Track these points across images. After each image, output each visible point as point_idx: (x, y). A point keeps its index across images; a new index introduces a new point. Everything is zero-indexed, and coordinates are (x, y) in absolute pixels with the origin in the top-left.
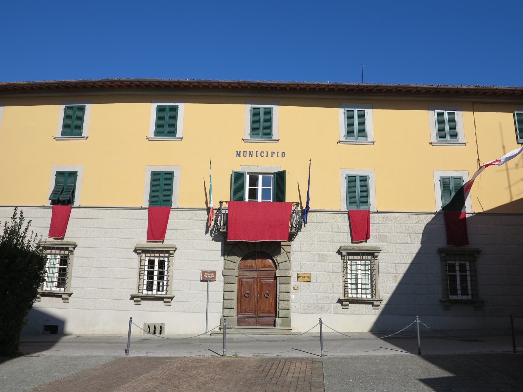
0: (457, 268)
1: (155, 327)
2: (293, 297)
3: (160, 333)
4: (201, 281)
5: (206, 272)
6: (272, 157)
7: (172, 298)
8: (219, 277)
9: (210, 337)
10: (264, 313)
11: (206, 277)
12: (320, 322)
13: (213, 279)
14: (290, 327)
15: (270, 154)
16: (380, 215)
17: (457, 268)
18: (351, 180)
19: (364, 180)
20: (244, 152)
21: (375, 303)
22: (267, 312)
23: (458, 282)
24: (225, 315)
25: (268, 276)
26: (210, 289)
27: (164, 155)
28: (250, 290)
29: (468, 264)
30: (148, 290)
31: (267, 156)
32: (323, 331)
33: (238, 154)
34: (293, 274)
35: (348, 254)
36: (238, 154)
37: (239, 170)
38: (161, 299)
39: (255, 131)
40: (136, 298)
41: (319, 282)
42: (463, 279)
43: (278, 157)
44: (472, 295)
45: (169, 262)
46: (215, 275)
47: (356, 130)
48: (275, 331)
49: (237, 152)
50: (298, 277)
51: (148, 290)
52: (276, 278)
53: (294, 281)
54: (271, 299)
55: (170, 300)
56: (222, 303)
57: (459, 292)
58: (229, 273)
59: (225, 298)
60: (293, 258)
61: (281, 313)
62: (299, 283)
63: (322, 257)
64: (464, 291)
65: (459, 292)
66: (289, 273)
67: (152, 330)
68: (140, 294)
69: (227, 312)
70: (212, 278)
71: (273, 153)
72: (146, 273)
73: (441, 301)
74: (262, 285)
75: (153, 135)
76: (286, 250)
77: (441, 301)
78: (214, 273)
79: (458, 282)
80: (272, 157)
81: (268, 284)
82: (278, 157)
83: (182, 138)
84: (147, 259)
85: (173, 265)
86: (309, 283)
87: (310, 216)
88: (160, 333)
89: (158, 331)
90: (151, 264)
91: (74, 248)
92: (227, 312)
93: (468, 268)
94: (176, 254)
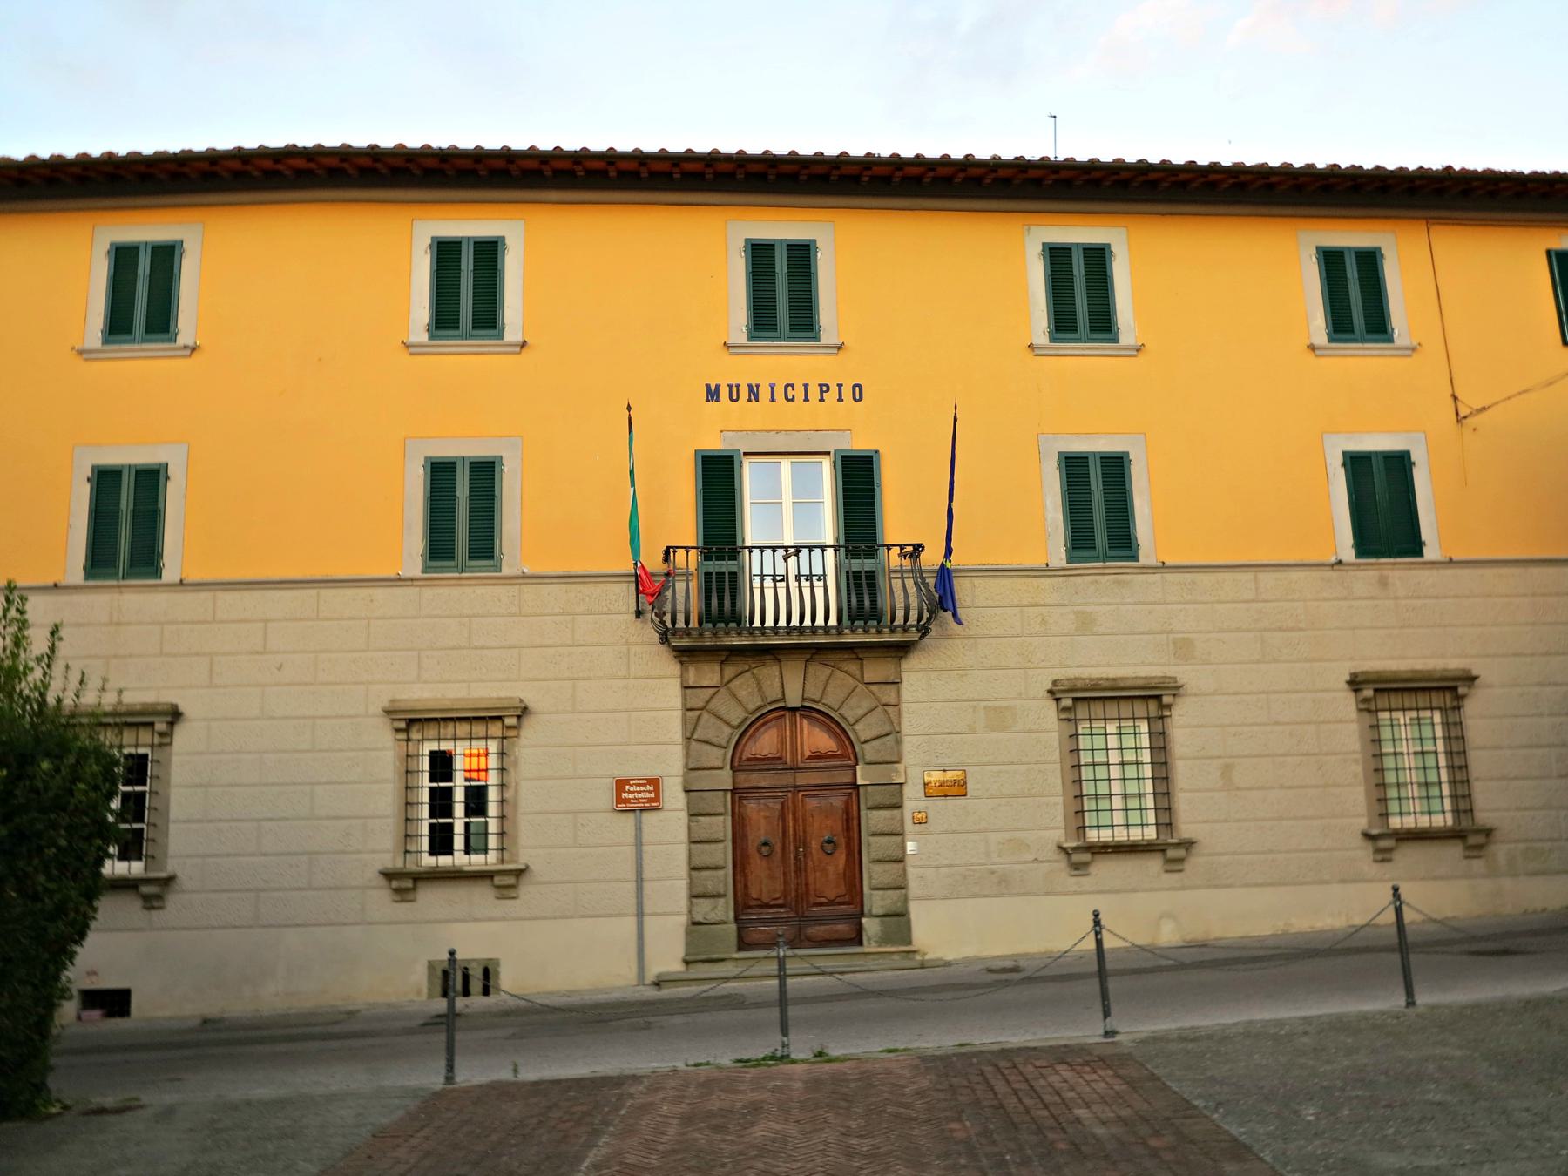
2: (910, 847)
5: (626, 782)
6: (822, 400)
7: (519, 873)
8: (674, 795)
9: (652, 994)
10: (821, 904)
12: (1097, 923)
14: (910, 943)
15: (814, 392)
16: (1172, 577)
19: (1116, 466)
20: (730, 386)
21: (1171, 853)
22: (831, 903)
24: (699, 918)
30: (434, 851)
31: (806, 399)
32: (1107, 945)
33: (713, 394)
36: (713, 394)
37: (714, 444)
39: (762, 321)
41: (991, 797)
43: (840, 399)
46: (657, 791)
48: (858, 962)
49: (708, 386)
55: (511, 880)
58: (704, 781)
59: (697, 862)
60: (906, 727)
62: (931, 802)
63: (999, 718)
66: (897, 771)
69: (704, 909)
70: (650, 800)
71: (824, 388)
73: (1367, 836)
78: (655, 782)
80: (822, 400)
82: (840, 399)
83: (524, 344)
85: (516, 763)
86: (961, 801)
88: (486, 992)
89: (476, 985)
91: (172, 724)
92: (704, 909)
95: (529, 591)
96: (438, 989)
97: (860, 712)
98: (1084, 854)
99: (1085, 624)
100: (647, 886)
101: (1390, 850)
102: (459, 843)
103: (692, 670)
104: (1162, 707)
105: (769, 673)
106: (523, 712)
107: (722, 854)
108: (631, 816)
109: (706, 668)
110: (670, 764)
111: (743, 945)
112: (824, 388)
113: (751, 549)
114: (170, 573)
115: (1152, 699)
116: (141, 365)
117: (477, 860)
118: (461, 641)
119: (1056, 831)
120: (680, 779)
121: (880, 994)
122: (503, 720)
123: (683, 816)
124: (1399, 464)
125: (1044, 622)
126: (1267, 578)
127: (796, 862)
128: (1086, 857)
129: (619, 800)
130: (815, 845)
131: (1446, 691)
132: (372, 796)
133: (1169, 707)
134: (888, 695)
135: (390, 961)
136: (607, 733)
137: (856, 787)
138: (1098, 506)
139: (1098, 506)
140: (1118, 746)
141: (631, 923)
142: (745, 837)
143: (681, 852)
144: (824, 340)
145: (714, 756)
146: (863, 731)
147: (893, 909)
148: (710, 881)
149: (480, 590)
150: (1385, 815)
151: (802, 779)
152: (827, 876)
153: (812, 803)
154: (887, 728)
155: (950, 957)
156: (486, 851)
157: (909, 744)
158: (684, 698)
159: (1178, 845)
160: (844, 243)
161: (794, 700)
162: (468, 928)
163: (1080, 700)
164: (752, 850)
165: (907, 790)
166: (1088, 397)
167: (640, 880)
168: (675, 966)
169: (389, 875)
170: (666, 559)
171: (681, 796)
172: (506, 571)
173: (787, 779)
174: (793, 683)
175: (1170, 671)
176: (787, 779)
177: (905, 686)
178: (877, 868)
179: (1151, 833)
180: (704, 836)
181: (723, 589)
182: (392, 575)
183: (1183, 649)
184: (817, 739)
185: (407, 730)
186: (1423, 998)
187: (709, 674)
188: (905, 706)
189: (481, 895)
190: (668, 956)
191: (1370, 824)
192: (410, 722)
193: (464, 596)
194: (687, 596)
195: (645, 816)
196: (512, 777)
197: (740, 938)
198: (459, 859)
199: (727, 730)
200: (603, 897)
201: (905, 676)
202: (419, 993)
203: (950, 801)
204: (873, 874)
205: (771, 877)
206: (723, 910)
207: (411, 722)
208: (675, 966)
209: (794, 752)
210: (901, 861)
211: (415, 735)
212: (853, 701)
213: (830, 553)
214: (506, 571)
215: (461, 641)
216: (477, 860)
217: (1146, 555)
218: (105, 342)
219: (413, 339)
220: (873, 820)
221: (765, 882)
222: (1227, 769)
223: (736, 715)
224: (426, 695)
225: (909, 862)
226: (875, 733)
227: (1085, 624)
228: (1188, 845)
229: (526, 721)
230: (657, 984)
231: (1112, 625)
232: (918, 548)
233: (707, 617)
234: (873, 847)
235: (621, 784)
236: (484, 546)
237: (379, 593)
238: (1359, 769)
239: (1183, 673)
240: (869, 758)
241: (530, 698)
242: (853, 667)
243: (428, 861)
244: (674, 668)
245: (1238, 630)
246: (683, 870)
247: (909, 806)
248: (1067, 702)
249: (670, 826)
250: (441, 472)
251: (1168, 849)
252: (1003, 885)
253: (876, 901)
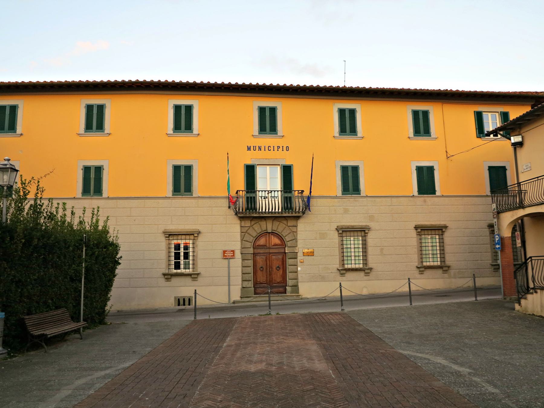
1: (184, 299)
2: (299, 269)
3: (189, 304)
5: (226, 251)
7: (198, 274)
8: (238, 255)
9: (233, 305)
11: (228, 255)
12: (340, 285)
15: (276, 148)
16: (369, 199)
18: (344, 169)
19: (355, 169)
21: (366, 271)
33: (249, 149)
36: (249, 149)
37: (249, 163)
39: (262, 129)
40: (168, 276)
45: (193, 244)
46: (234, 253)
51: (185, 268)
53: (300, 257)
55: (196, 276)
58: (246, 251)
59: (244, 272)
60: (299, 237)
62: (304, 257)
63: (323, 236)
67: (182, 302)
68: (170, 273)
69: (246, 284)
72: (173, 254)
73: (417, 267)
75: (171, 132)
76: (293, 230)
83: (198, 135)
85: (197, 246)
86: (312, 257)
87: (313, 202)
88: (189, 304)
89: (187, 303)
90: (177, 247)
92: (246, 284)
95: (200, 201)
96: (177, 304)
97: (287, 234)
98: (344, 271)
99: (346, 211)
100: (231, 278)
101: (423, 271)
102: (182, 266)
103: (243, 222)
104: (365, 233)
106: (199, 233)
107: (250, 270)
108: (226, 261)
109: (247, 222)
110: (237, 246)
111: (255, 293)
113: (259, 191)
114: (105, 195)
115: (362, 231)
116: (94, 138)
117: (187, 271)
118: (183, 214)
119: (336, 264)
120: (239, 251)
121: (290, 304)
122: (194, 234)
123: (240, 260)
124: (431, 170)
125: (335, 210)
126: (394, 200)
127: (270, 272)
128: (344, 272)
129: (224, 256)
130: (274, 268)
131: (440, 230)
132: (160, 254)
133: (367, 233)
134: (294, 229)
135: (165, 296)
136: (221, 238)
137: (285, 253)
138: (350, 179)
139: (350, 179)
140: (354, 243)
141: (227, 287)
142: (256, 266)
143: (240, 269)
144: (279, 134)
145: (249, 245)
146: (287, 239)
147: (294, 284)
148: (247, 277)
149: (187, 200)
150: (422, 262)
151: (271, 251)
152: (277, 276)
153: (274, 257)
154: (294, 238)
155: (308, 297)
156: (189, 269)
157: (299, 242)
158: (241, 229)
159: (368, 269)
160: (284, 107)
161: (269, 230)
162: (185, 289)
163: (344, 231)
164: (258, 269)
165: (299, 254)
166: (348, 151)
167: (229, 277)
168: (238, 299)
169: (164, 275)
170: (237, 193)
171: (240, 255)
172: (194, 196)
173: (267, 251)
174: (269, 226)
175: (368, 224)
176: (267, 251)
177: (298, 227)
178: (290, 274)
179: (361, 266)
180: (246, 265)
181: (251, 201)
182: (164, 196)
183: (371, 218)
184: (275, 240)
185: (168, 237)
186: (413, 304)
187: (248, 223)
188: (298, 232)
189: (188, 280)
190: (236, 296)
191: (418, 264)
192: (169, 235)
193: (183, 202)
194: (242, 203)
195: (231, 260)
196: (196, 249)
197: (255, 291)
198: (182, 270)
199: (252, 238)
200: (220, 282)
201: (298, 224)
202: (172, 305)
203: (310, 257)
204: (289, 275)
205: (263, 276)
206: (250, 284)
207: (170, 235)
208: (238, 299)
209: (269, 243)
210: (297, 272)
211: (170, 239)
212: (285, 231)
213: (280, 192)
214: (194, 196)
215: (183, 214)
216: (187, 271)
217: (363, 194)
218: (85, 132)
219: (169, 133)
220: (290, 262)
221: (262, 278)
222: (382, 250)
223: (254, 234)
224: (174, 228)
225: (299, 272)
226: (290, 239)
227: (346, 211)
228: (371, 269)
229: (199, 235)
230: (234, 303)
231: (353, 212)
232: (303, 191)
233: (247, 208)
234: (289, 269)
235: (224, 252)
236: (188, 189)
237: (161, 201)
238: (416, 250)
239: (372, 225)
240: (289, 246)
241: (200, 228)
242: (285, 222)
243: (175, 271)
244: (238, 222)
245: (386, 213)
246: (240, 274)
247: (299, 258)
248: (341, 232)
249: (237, 263)
250: (177, 169)
251: (366, 270)
252: (323, 279)
253: (290, 282)
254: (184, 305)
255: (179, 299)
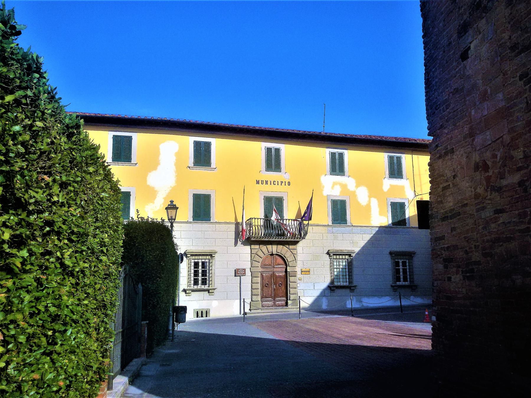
0: (401, 264)
1: (202, 312)
3: (206, 316)
4: (235, 276)
8: (248, 273)
11: (239, 273)
13: (244, 274)
15: (280, 183)
17: (401, 264)
21: (352, 288)
23: (401, 274)
25: (281, 272)
26: (242, 282)
27: (202, 181)
28: (268, 281)
29: (407, 261)
33: (258, 182)
34: (298, 269)
35: (334, 255)
36: (258, 182)
38: (208, 291)
42: (405, 271)
44: (410, 281)
47: (337, 167)
50: (302, 272)
52: (286, 271)
53: (299, 275)
54: (283, 288)
56: (250, 292)
57: (402, 280)
58: (253, 270)
61: (292, 297)
64: (405, 280)
65: (402, 280)
67: (200, 315)
71: (282, 182)
73: (392, 286)
74: (277, 277)
77: (392, 286)
78: (245, 270)
79: (401, 274)
81: (280, 277)
84: (193, 261)
88: (206, 316)
89: (204, 315)
90: (196, 265)
93: (407, 264)
94: (216, 256)
105: (270, 247)
110: (247, 265)
111: (263, 306)
112: (282, 182)
122: (211, 255)
131: (410, 255)
157: (298, 262)
159: (353, 286)
191: (393, 283)
195: (242, 277)
198: (200, 286)
220: (292, 279)
249: (247, 280)
254: (202, 316)
255: (197, 312)
